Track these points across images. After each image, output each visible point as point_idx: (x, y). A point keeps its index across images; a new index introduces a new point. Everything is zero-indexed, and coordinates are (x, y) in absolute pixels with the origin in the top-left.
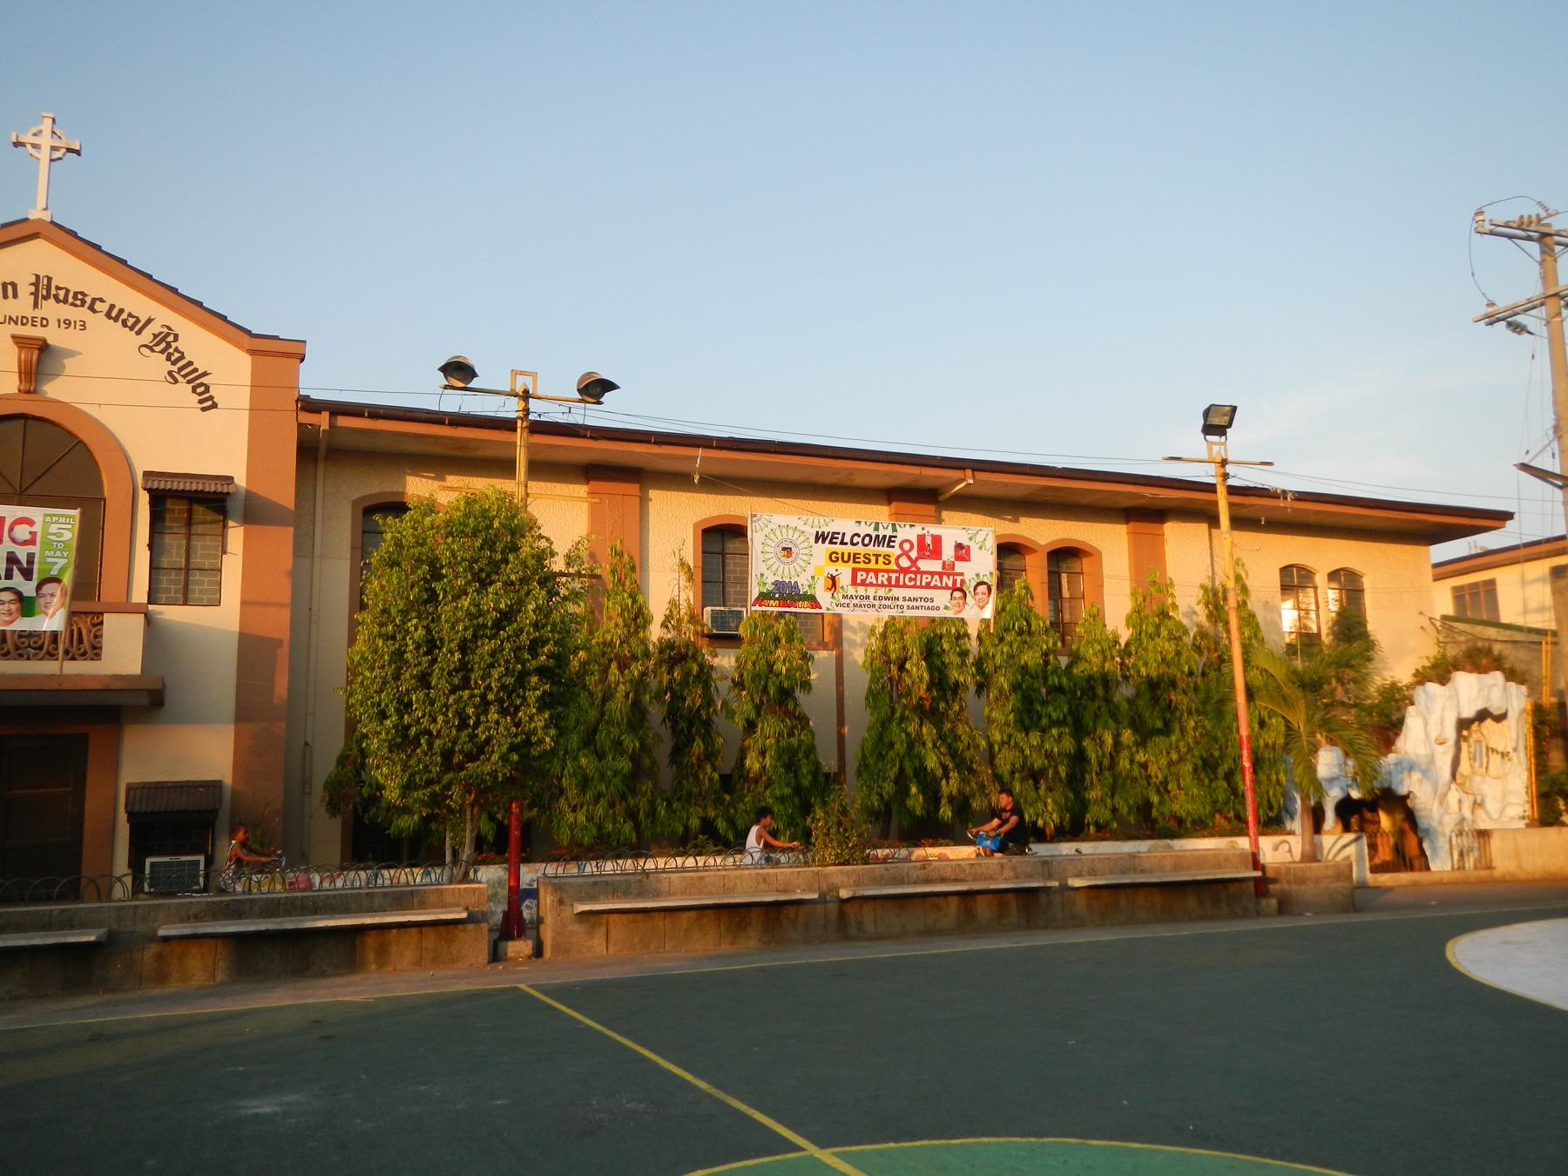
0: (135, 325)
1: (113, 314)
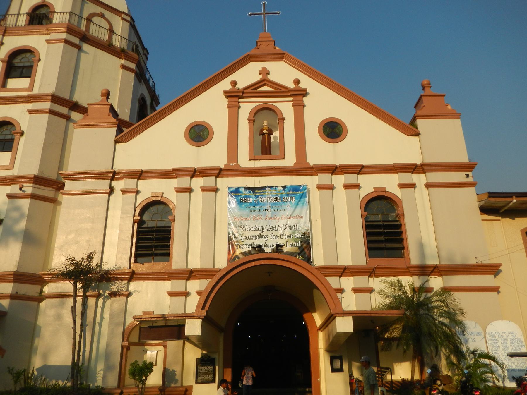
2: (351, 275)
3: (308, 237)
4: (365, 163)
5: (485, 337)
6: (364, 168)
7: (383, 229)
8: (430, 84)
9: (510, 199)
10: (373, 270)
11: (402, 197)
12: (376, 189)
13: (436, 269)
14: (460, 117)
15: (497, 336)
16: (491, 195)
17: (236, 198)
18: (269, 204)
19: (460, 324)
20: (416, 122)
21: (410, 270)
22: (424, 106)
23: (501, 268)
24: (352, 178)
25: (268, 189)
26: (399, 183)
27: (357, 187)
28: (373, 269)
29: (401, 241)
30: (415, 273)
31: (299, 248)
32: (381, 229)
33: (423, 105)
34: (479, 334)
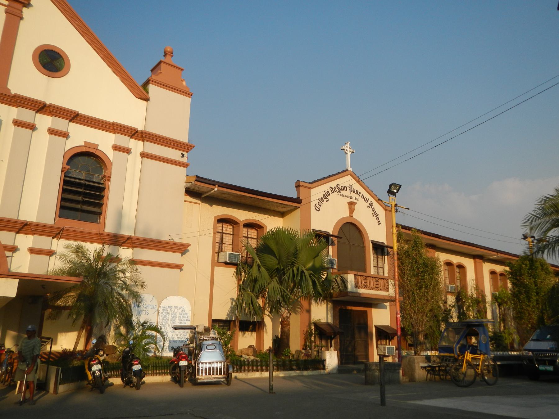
0: (367, 201)
1: (363, 197)
2: (31, 232)
4: (82, 111)
5: (158, 310)
6: (79, 117)
7: (83, 189)
8: (172, 54)
9: (212, 187)
10: (61, 231)
11: (113, 160)
12: (87, 144)
13: (129, 240)
14: (192, 96)
15: (169, 310)
16: (199, 179)
19: (136, 295)
20: (148, 86)
21: (102, 237)
22: (161, 73)
23: (189, 248)
24: (61, 124)
26: (114, 144)
27: (66, 135)
28: (60, 230)
29: (100, 205)
30: (107, 242)
32: (81, 188)
33: (160, 71)
34: (153, 307)
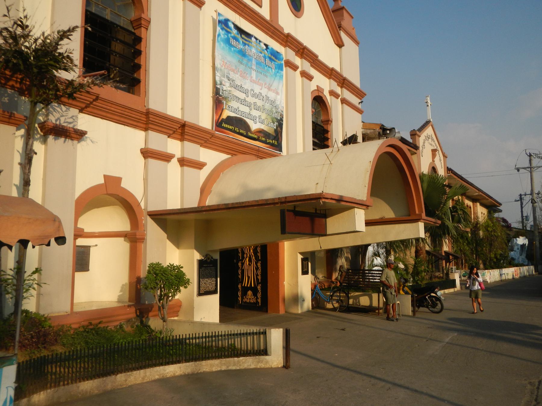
3: (281, 120)
17: (227, 33)
18: (254, 62)
25: (253, 39)
31: (276, 131)
